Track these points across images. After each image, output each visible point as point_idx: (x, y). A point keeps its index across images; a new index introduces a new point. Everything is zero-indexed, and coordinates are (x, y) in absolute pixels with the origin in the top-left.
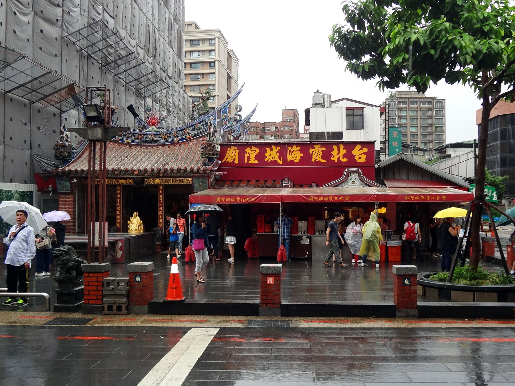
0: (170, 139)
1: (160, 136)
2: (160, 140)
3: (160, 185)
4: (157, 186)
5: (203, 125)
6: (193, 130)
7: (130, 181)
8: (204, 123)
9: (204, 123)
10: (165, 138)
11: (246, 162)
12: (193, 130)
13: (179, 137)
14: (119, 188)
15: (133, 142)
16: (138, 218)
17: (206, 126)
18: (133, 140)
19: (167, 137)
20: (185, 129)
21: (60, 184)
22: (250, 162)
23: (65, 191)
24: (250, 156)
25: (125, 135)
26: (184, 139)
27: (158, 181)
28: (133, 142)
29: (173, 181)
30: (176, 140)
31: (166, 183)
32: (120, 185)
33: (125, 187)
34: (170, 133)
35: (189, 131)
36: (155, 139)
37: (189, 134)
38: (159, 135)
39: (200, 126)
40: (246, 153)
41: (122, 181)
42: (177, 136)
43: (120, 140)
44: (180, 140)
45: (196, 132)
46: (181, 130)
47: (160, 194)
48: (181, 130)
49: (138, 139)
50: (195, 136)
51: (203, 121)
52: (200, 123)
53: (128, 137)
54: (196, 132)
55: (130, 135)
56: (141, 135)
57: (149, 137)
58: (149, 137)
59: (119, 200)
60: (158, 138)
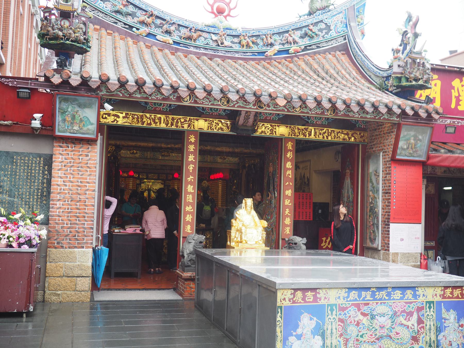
0: (255, 48)
1: (236, 40)
2: (237, 47)
3: (288, 139)
4: (276, 143)
5: (321, 30)
6: (302, 37)
7: (221, 127)
8: (322, 26)
9: (322, 26)
10: (248, 46)
11: (453, 106)
12: (302, 37)
13: (277, 47)
14: (193, 139)
15: (178, 44)
16: (254, 213)
17: (327, 33)
18: (177, 39)
19: (251, 44)
20: (287, 32)
21: (63, 112)
22: (460, 108)
23: (77, 132)
24: (459, 95)
25: (160, 26)
26: (287, 51)
27: (282, 131)
28: (178, 44)
29: (315, 133)
30: (271, 52)
31: (301, 137)
32: (194, 132)
33: (205, 138)
34: (258, 36)
35: (297, 39)
36: (226, 43)
37: (295, 42)
38: (234, 36)
39: (315, 29)
40: (453, 88)
41: (201, 124)
42: (272, 45)
43: (149, 35)
44: (280, 52)
45: (306, 41)
46: (279, 34)
47: (288, 160)
48: (279, 34)
49: (189, 38)
50: (306, 49)
51: (321, 21)
52: (316, 24)
53: (168, 32)
54: (306, 41)
55: (173, 28)
56: (196, 30)
57: (214, 37)
58: (214, 37)
59: (191, 167)
60: (232, 42)
